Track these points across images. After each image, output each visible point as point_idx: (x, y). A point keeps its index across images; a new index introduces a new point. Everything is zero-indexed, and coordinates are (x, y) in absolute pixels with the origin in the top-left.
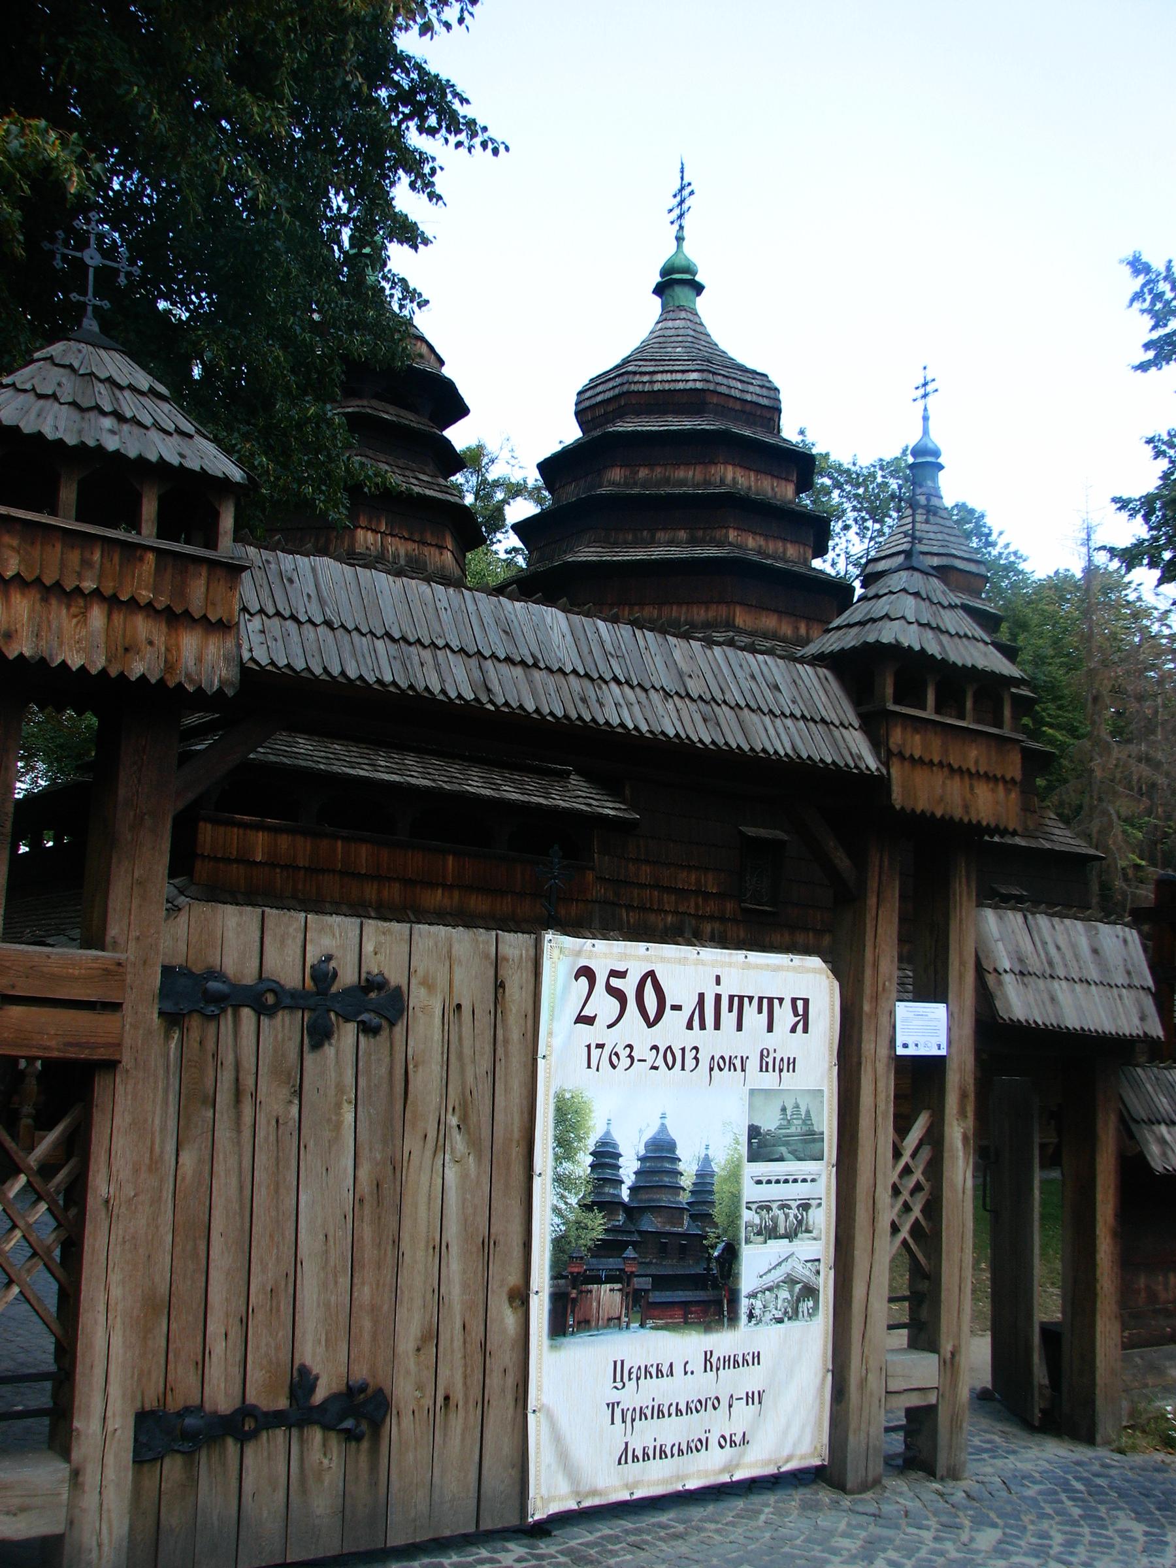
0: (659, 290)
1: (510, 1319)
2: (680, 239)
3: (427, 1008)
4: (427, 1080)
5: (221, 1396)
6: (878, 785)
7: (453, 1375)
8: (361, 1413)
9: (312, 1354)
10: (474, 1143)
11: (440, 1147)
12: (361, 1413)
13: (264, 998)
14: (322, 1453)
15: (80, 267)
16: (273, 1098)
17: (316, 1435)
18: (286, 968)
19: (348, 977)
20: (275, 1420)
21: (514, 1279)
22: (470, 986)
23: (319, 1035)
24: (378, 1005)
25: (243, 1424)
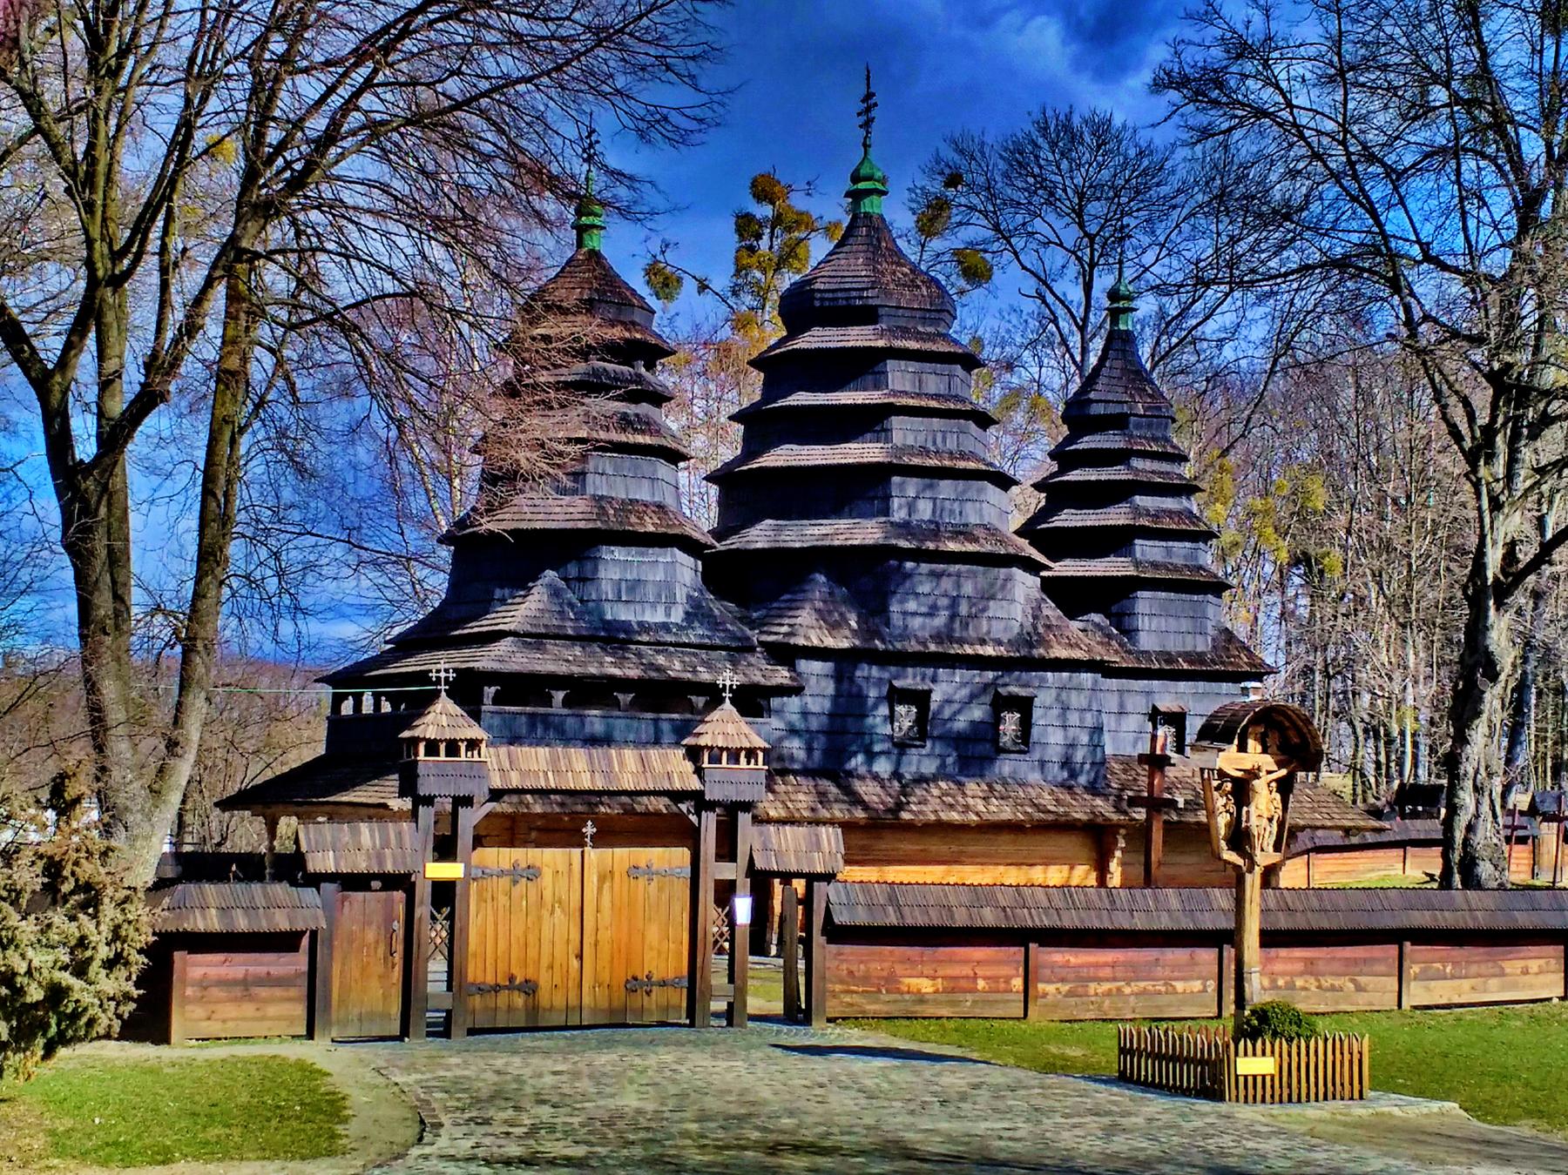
0: (848, 195)
1: (575, 963)
2: (866, 146)
3: (547, 875)
4: (548, 895)
5: (490, 980)
6: (702, 793)
7: (557, 980)
8: (529, 988)
9: (514, 971)
10: (563, 911)
11: (552, 913)
12: (529, 988)
13: (502, 873)
14: (519, 1000)
15: (438, 678)
16: (503, 900)
17: (516, 993)
18: (506, 866)
19: (524, 865)
20: (506, 987)
21: (577, 951)
22: (562, 868)
23: (515, 882)
24: (532, 873)
25: (497, 988)
